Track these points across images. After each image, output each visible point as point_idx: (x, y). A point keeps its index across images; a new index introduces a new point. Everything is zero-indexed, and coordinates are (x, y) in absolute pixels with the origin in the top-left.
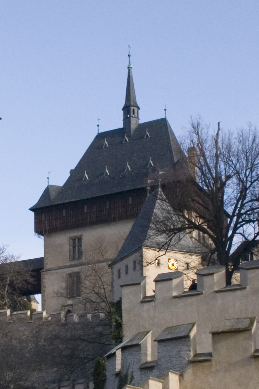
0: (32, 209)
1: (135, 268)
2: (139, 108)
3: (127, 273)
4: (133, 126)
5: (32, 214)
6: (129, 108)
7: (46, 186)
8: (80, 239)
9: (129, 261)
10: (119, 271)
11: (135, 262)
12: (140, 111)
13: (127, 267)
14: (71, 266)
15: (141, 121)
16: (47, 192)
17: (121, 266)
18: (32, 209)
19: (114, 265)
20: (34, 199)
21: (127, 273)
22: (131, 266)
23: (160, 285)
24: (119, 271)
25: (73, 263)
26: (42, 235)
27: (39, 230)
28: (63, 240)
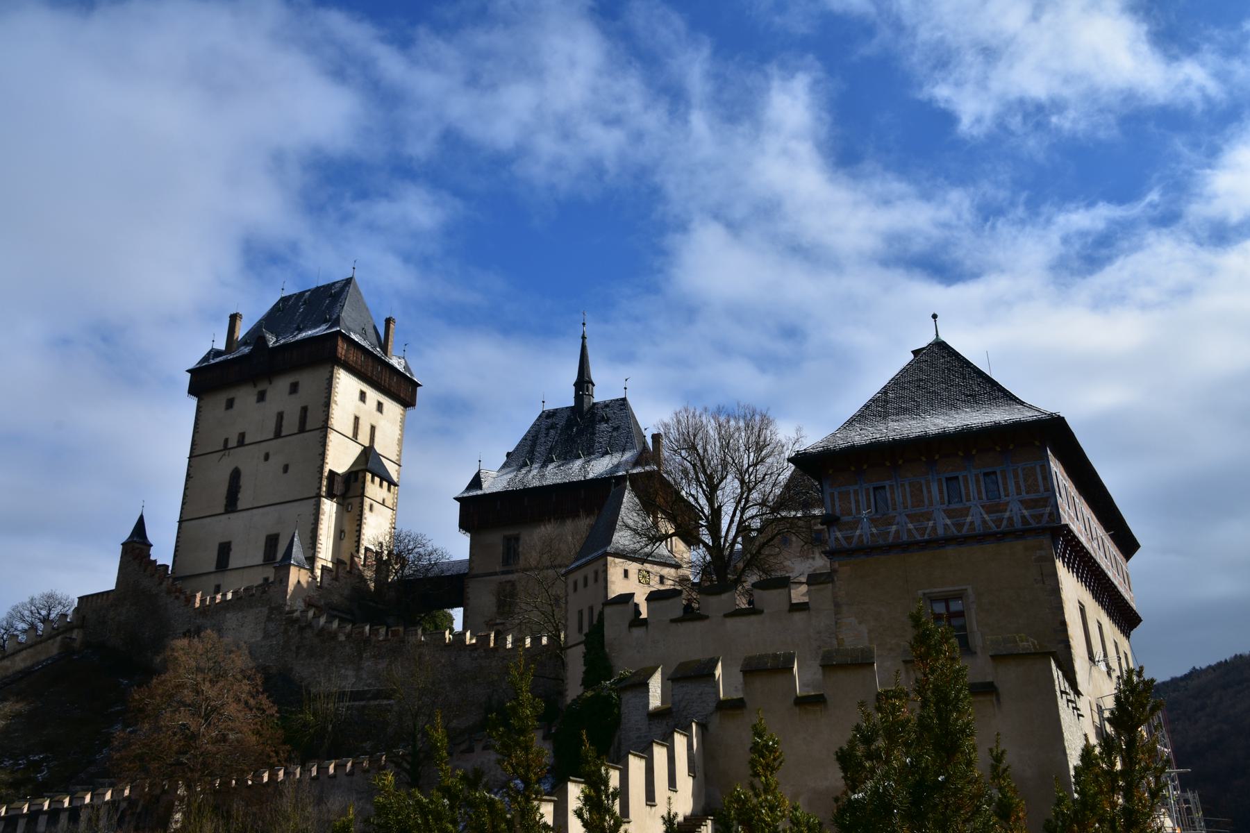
1: (596, 580)
3: (586, 585)
4: (586, 407)
6: (583, 383)
8: (517, 539)
9: (589, 571)
10: (575, 583)
11: (596, 573)
14: (503, 573)
15: (595, 400)
17: (579, 576)
21: (586, 585)
22: (591, 577)
23: (657, 604)
24: (575, 583)
25: (506, 569)
27: (464, 525)
28: (496, 539)
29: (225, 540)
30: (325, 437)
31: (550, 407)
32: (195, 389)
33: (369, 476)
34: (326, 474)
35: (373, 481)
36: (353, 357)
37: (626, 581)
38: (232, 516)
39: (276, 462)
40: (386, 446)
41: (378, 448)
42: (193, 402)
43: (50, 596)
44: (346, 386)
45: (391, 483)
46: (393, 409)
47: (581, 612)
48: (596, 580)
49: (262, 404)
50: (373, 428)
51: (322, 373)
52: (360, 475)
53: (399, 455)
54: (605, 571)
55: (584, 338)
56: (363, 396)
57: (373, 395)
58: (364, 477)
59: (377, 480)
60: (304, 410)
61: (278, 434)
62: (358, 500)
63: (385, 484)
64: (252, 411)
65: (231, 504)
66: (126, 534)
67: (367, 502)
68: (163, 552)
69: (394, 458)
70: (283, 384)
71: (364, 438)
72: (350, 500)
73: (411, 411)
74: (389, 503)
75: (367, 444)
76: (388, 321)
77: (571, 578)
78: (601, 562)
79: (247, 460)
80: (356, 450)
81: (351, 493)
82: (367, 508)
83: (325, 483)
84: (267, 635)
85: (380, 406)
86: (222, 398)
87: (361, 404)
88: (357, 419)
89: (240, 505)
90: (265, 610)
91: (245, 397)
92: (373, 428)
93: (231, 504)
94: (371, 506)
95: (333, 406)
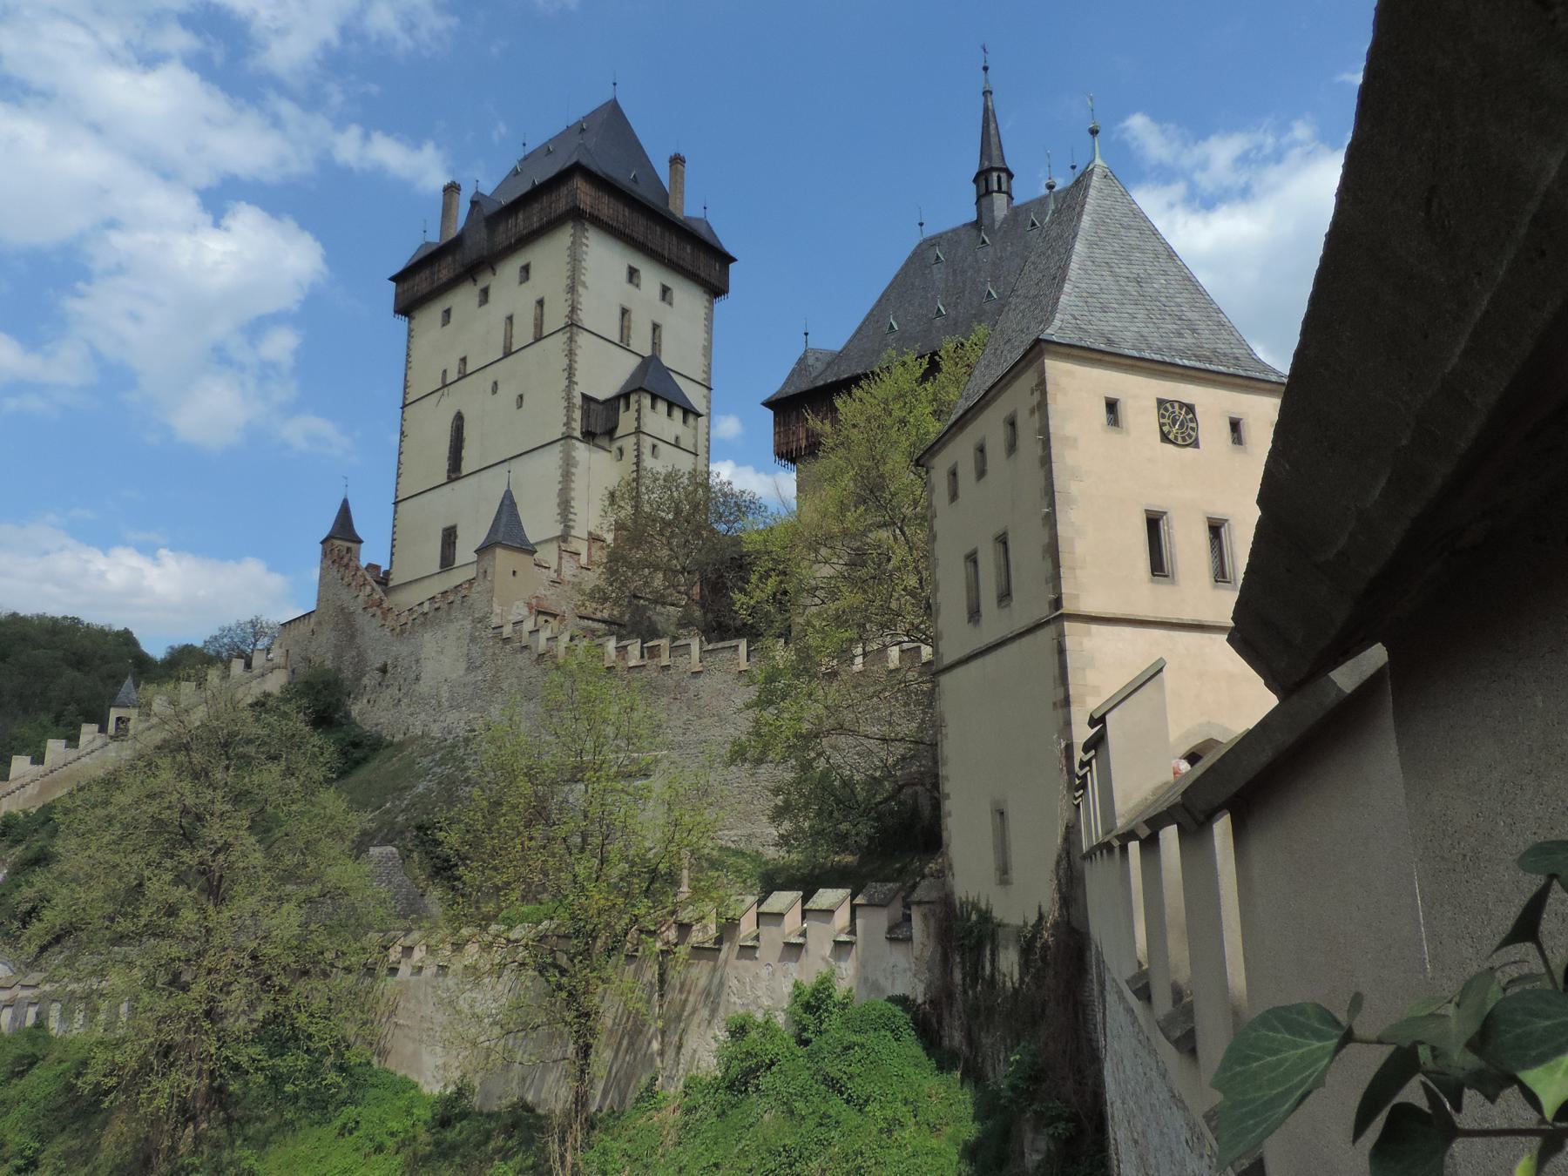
0: (769, 404)
1: (1012, 447)
2: (1010, 176)
3: (981, 473)
5: (771, 413)
6: (990, 177)
7: (800, 353)
9: (989, 427)
10: (953, 474)
12: (1014, 181)
13: (981, 450)
16: (802, 365)
17: (960, 452)
18: (769, 404)
19: (933, 455)
20: (774, 383)
21: (981, 473)
24: (953, 474)
26: (793, 461)
29: (449, 524)
30: (571, 339)
31: (931, 231)
32: (407, 308)
33: (647, 401)
34: (578, 401)
35: (653, 407)
36: (607, 207)
37: (1114, 436)
38: (457, 485)
39: (508, 393)
40: (680, 356)
41: (666, 360)
42: (402, 323)
43: (253, 624)
44: (604, 259)
45: (689, 412)
46: (688, 298)
47: (972, 558)
48: (1012, 447)
49: (485, 308)
50: (656, 327)
51: (562, 239)
52: (633, 398)
53: (708, 370)
54: (1042, 407)
55: (987, 93)
56: (633, 273)
57: (652, 277)
58: (638, 401)
59: (662, 407)
60: (541, 303)
61: (508, 353)
62: (633, 439)
63: (678, 414)
64: (473, 321)
65: (455, 469)
66: (326, 528)
67: (647, 442)
68: (373, 551)
69: (700, 377)
70: (509, 270)
71: (641, 342)
72: (618, 444)
73: (721, 304)
74: (686, 442)
75: (647, 352)
76: (677, 161)
77: (941, 464)
78: (1028, 379)
79: (470, 398)
80: (633, 363)
81: (619, 432)
82: (646, 451)
83: (577, 414)
84: (471, 667)
85: (665, 291)
86: (434, 312)
87: (631, 288)
88: (625, 312)
89: (465, 470)
90: (467, 625)
91: (463, 299)
92: (656, 327)
93: (455, 469)
94: (654, 447)
95: (581, 289)
